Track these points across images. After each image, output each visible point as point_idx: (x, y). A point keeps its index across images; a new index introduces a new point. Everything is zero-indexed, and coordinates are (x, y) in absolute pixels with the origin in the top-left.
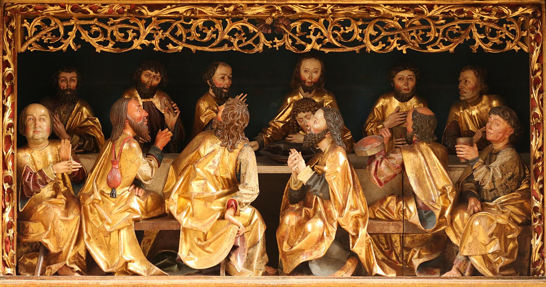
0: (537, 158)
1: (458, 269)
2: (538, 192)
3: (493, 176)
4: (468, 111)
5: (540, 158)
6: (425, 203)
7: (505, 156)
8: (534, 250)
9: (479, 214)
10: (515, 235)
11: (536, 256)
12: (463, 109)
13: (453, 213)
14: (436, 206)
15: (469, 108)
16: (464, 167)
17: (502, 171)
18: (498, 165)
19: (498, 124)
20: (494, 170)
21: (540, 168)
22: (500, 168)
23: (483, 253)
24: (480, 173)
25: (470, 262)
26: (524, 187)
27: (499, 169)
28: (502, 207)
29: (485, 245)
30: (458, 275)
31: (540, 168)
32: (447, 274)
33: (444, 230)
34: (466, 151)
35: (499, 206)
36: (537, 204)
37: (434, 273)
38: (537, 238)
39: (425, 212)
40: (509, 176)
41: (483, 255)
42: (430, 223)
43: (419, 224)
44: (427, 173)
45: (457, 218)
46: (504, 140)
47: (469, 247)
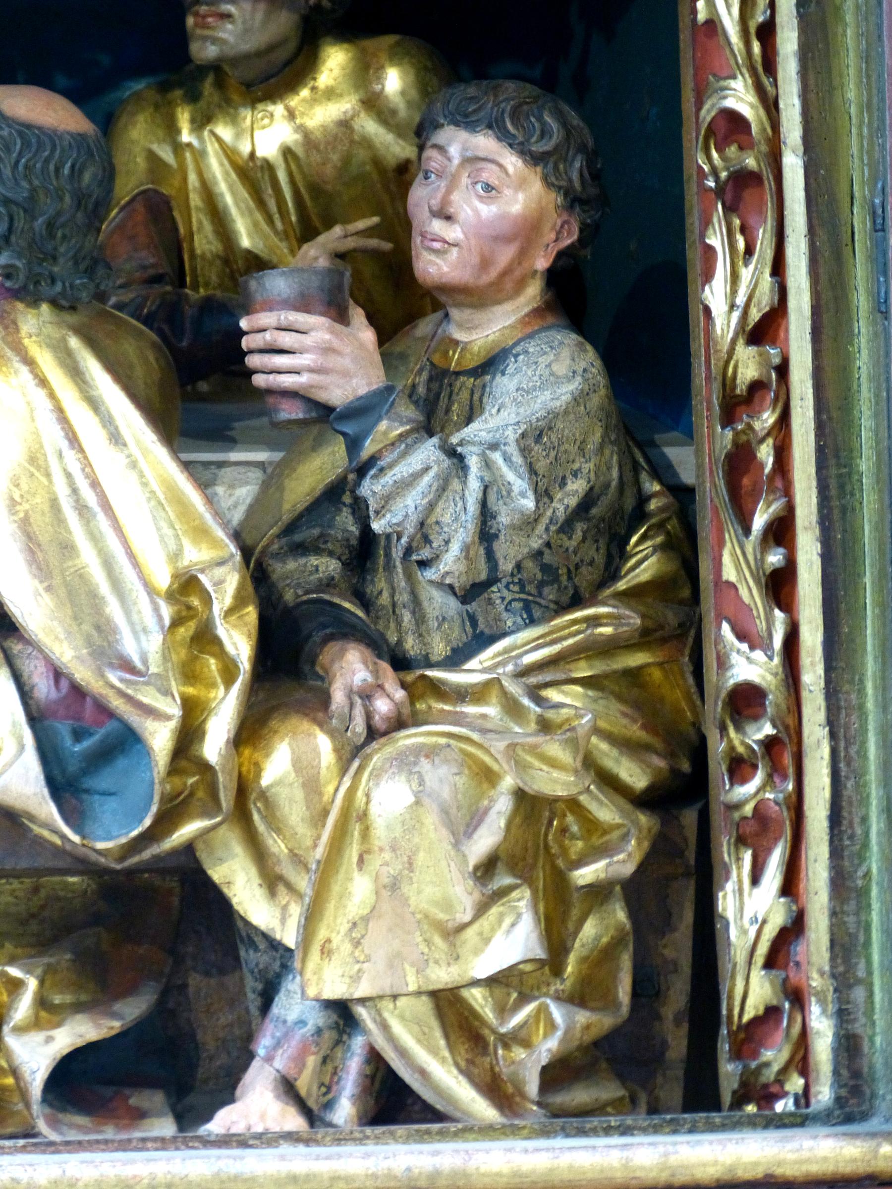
0: (741, 388)
1: (288, 1088)
2: (751, 594)
3: (484, 504)
4: (224, 131)
5: (757, 386)
6: (83, 674)
7: (543, 381)
8: (739, 955)
9: (408, 738)
10: (622, 863)
11: (752, 991)
12: (201, 122)
13: (250, 732)
14: (149, 697)
15: (234, 121)
16: (261, 465)
17: (532, 470)
18: (511, 435)
19: (488, 188)
20: (487, 464)
21: (766, 454)
22: (524, 451)
23: (442, 976)
24: (406, 487)
25: (358, 1043)
26: (645, 563)
27: (518, 459)
28: (534, 693)
29: (453, 933)
30: (295, 1122)
31: (766, 454)
32: (223, 1121)
33: (189, 849)
34: (308, 349)
35: (514, 688)
36: (750, 667)
37: (139, 1115)
38: (755, 880)
39: (78, 735)
40: (573, 502)
41: (435, 995)
42: (112, 804)
43: (49, 810)
44: (75, 491)
45: (277, 765)
46: (520, 286)
47: (357, 944)
